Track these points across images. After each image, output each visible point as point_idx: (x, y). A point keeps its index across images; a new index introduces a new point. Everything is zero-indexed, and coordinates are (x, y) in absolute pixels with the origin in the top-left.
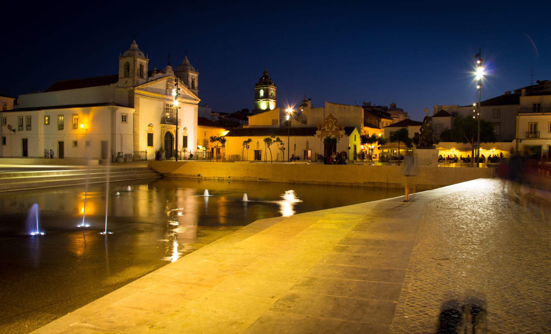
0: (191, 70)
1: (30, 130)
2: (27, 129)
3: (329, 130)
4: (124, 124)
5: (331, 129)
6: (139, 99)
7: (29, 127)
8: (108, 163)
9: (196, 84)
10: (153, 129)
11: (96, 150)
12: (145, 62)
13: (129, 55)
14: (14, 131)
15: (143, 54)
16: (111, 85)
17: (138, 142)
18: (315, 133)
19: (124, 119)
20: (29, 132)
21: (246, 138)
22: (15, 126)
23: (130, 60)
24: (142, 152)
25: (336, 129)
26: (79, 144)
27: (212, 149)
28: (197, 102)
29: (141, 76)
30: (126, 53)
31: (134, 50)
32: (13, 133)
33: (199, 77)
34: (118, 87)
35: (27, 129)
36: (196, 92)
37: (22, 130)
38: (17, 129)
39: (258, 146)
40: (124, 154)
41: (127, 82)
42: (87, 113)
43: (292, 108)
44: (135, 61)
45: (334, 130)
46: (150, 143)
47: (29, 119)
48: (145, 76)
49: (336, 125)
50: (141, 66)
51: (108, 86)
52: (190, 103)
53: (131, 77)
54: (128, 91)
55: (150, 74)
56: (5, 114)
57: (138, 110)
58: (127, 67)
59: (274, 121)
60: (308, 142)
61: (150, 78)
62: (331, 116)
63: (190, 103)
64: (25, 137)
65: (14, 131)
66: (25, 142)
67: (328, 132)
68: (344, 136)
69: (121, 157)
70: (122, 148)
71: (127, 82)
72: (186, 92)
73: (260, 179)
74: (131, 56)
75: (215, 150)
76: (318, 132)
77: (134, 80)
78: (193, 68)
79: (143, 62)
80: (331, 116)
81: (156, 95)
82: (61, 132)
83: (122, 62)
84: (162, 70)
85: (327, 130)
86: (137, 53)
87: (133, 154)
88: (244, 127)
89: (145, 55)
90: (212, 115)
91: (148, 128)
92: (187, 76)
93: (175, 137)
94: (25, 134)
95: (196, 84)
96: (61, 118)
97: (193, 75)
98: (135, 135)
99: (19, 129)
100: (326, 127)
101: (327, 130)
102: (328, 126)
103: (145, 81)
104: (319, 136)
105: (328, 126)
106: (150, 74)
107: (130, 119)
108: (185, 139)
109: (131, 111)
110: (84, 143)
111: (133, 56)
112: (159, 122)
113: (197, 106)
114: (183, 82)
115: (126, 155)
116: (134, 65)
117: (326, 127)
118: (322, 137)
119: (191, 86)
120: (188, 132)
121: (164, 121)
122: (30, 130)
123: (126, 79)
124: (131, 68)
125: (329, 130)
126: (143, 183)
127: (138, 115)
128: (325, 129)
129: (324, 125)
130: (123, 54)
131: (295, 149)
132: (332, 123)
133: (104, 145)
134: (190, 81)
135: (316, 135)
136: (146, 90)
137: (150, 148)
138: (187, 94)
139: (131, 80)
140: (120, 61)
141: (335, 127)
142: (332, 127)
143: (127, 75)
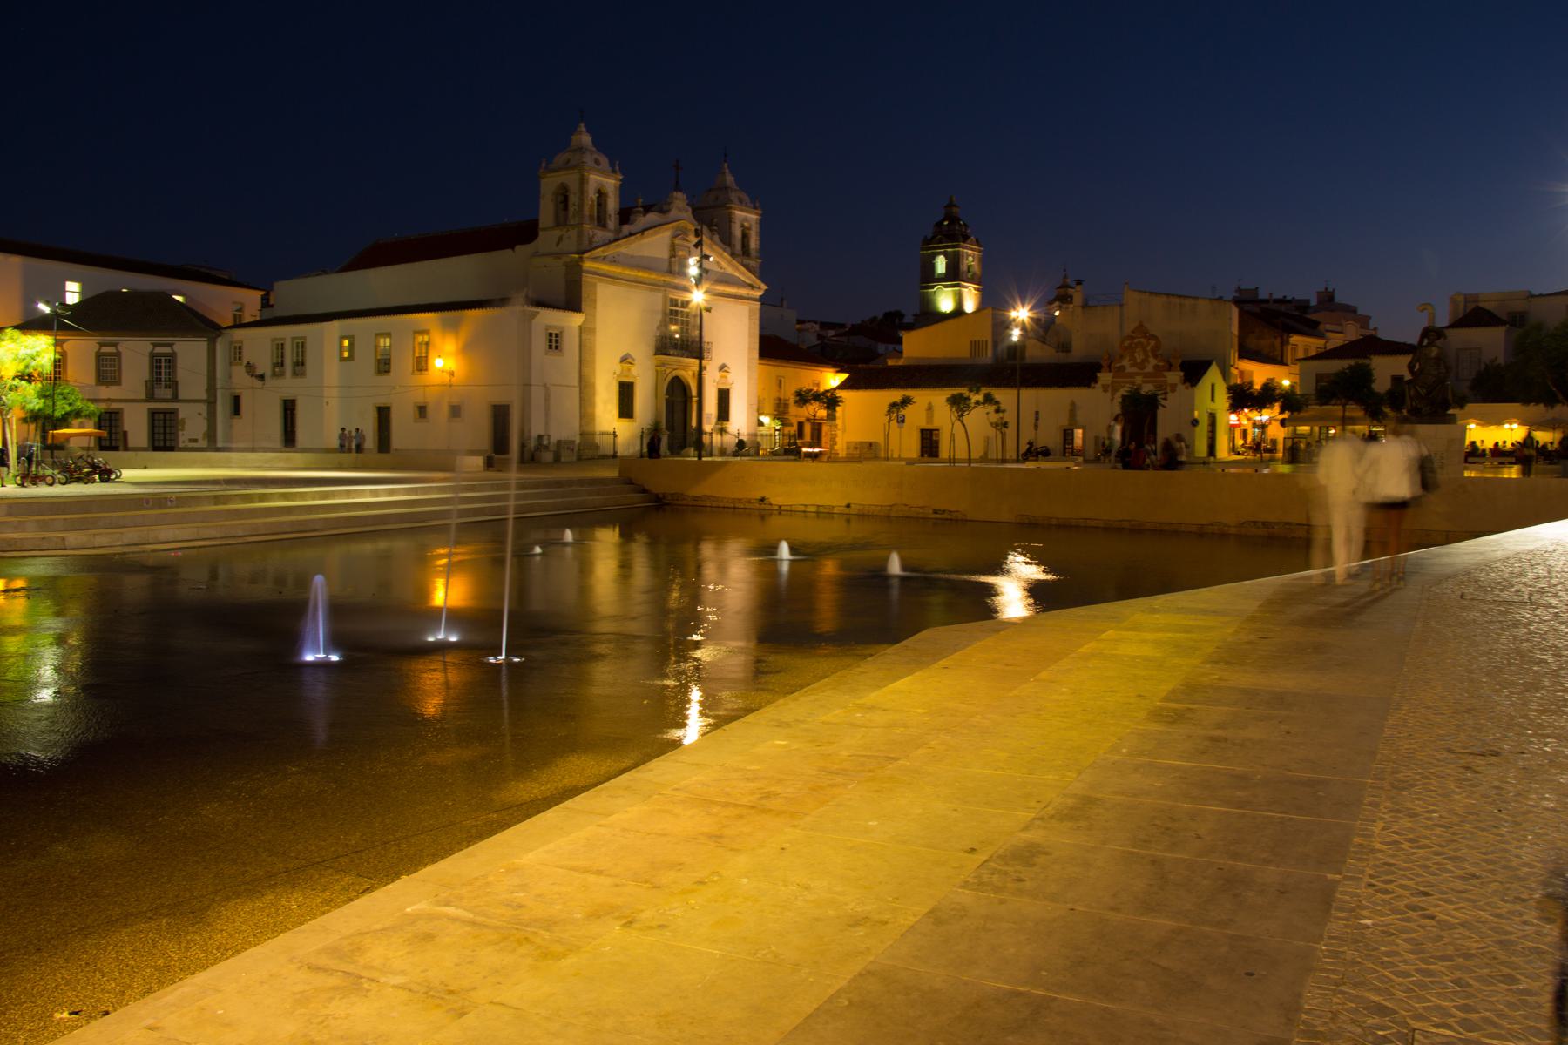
0: (741, 201)
1: (303, 374)
2: (295, 374)
3: (1134, 370)
5: (1141, 366)
6: (594, 285)
7: (300, 365)
8: (514, 465)
9: (754, 243)
10: (635, 370)
11: (478, 430)
12: (611, 183)
13: (567, 166)
14: (262, 377)
15: (604, 161)
16: (518, 248)
17: (593, 405)
18: (1095, 380)
19: (554, 341)
20: (298, 380)
21: (896, 395)
22: (264, 366)
23: (569, 178)
24: (603, 434)
25: (1156, 367)
26: (430, 412)
27: (801, 425)
28: (758, 294)
29: (601, 221)
30: (560, 159)
31: (581, 149)
32: (258, 383)
33: (763, 223)
34: (536, 254)
35: (295, 374)
36: (754, 263)
37: (282, 375)
38: (268, 373)
39: (930, 418)
40: (554, 439)
41: (560, 239)
42: (453, 327)
43: (1027, 308)
44: (583, 181)
45: (1149, 369)
46: (626, 410)
47: (301, 346)
48: (612, 223)
49: (1155, 356)
50: (601, 195)
51: (509, 251)
54: (566, 265)
55: (625, 216)
56: (239, 334)
57: (591, 319)
58: (561, 198)
59: (976, 346)
60: (1073, 404)
61: (626, 229)
62: (1141, 329)
64: (288, 395)
65: (262, 377)
66: (289, 408)
67: (1132, 375)
68: (1181, 387)
69: (546, 448)
70: (547, 424)
71: (560, 239)
72: (724, 264)
73: (935, 512)
74: (574, 167)
75: (807, 429)
76: (1105, 377)
77: (580, 234)
78: (746, 198)
79: (604, 181)
80: (1141, 329)
81: (641, 274)
82: (383, 379)
83: (549, 185)
84: (656, 205)
85: (1129, 370)
86: (588, 160)
88: (890, 362)
89: (612, 165)
90: (799, 330)
91: (618, 368)
92: (730, 219)
93: (694, 392)
94: (288, 386)
95: (754, 243)
96: (385, 342)
97: (745, 217)
98: (585, 388)
99: (274, 374)
100: (1126, 362)
101: (1129, 370)
102: (1133, 358)
103: (610, 236)
104: (1105, 389)
105: (1133, 358)
106: (625, 216)
107: (571, 343)
108: (724, 397)
109: (576, 319)
110: (445, 410)
111: (579, 167)
112: (650, 350)
113: (757, 305)
114: (716, 237)
115: (559, 442)
116: (582, 191)
117: (1126, 362)
118: (1114, 391)
119: (738, 247)
120: (730, 377)
121: (664, 346)
122: (303, 374)
123: (557, 232)
124: (573, 199)
125: (1134, 370)
126: (604, 523)
127: (593, 331)
128: (1122, 368)
129: (1122, 357)
131: (1036, 426)
132: (1145, 351)
133: (500, 415)
134: (738, 233)
135: (1099, 385)
138: (730, 270)
139: (573, 233)
140: (543, 182)
141: (1153, 361)
142: (1145, 360)
143: (561, 222)
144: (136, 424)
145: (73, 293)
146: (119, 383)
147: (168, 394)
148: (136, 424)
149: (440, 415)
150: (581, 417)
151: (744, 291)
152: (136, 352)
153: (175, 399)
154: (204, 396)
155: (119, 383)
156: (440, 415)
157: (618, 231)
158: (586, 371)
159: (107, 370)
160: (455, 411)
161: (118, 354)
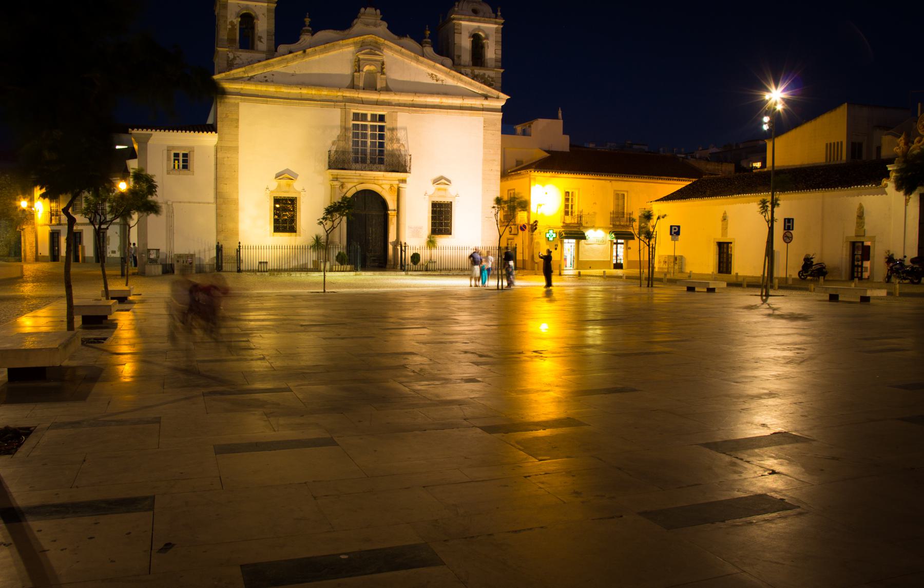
6: (237, 105)
9: (492, 52)
17: (235, 220)
19: (183, 161)
28: (500, 104)
36: (495, 73)
39: (725, 229)
43: (781, 88)
52: (461, 108)
63: (461, 108)
72: (441, 76)
81: (312, 92)
90: (356, 127)
91: (274, 184)
95: (492, 52)
98: (224, 206)
109: (208, 140)
113: (499, 116)
114: (429, 50)
119: (466, 57)
134: (466, 43)
136: (265, 80)
137: (284, 239)
138: (450, 82)
150: (219, 232)
151: (477, 102)
158: (226, 189)
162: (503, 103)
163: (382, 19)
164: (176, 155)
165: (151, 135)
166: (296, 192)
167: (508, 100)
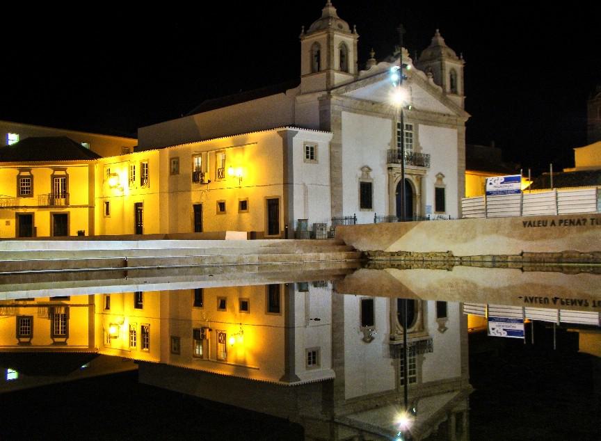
0: (449, 55)
4: (310, 165)
10: (371, 174)
11: (257, 217)
12: (351, 40)
13: (318, 30)
15: (346, 26)
16: (288, 91)
23: (321, 37)
26: (227, 207)
29: (344, 68)
30: (316, 24)
31: (329, 17)
33: (466, 70)
34: (299, 94)
40: (310, 223)
42: (240, 145)
44: (330, 39)
46: (366, 200)
53: (324, 71)
55: (362, 64)
57: (338, 137)
61: (363, 73)
74: (323, 30)
77: (329, 77)
78: (453, 53)
79: (345, 38)
83: (307, 42)
84: (386, 55)
86: (333, 24)
87: (329, 224)
88: (565, 170)
89: (351, 28)
91: (360, 173)
92: (442, 67)
93: (417, 192)
96: (198, 161)
97: (453, 65)
106: (362, 64)
107: (323, 153)
110: (236, 206)
111: (326, 28)
115: (315, 225)
116: (330, 47)
121: (396, 157)
126: (97, 236)
127: (340, 146)
130: (307, 29)
133: (272, 204)
140: (303, 42)
143: (316, 69)
144: (43, 222)
145: (13, 139)
146: (31, 196)
147: (62, 201)
148: (43, 222)
149: (233, 208)
152: (43, 176)
153: (67, 203)
154: (87, 203)
155: (31, 196)
156: (233, 208)
157: (357, 74)
159: (25, 188)
160: (243, 205)
161: (32, 176)
162: (466, 120)
163: (409, 56)
164: (307, 148)
165: (297, 132)
166: (371, 179)
167: (469, 118)
